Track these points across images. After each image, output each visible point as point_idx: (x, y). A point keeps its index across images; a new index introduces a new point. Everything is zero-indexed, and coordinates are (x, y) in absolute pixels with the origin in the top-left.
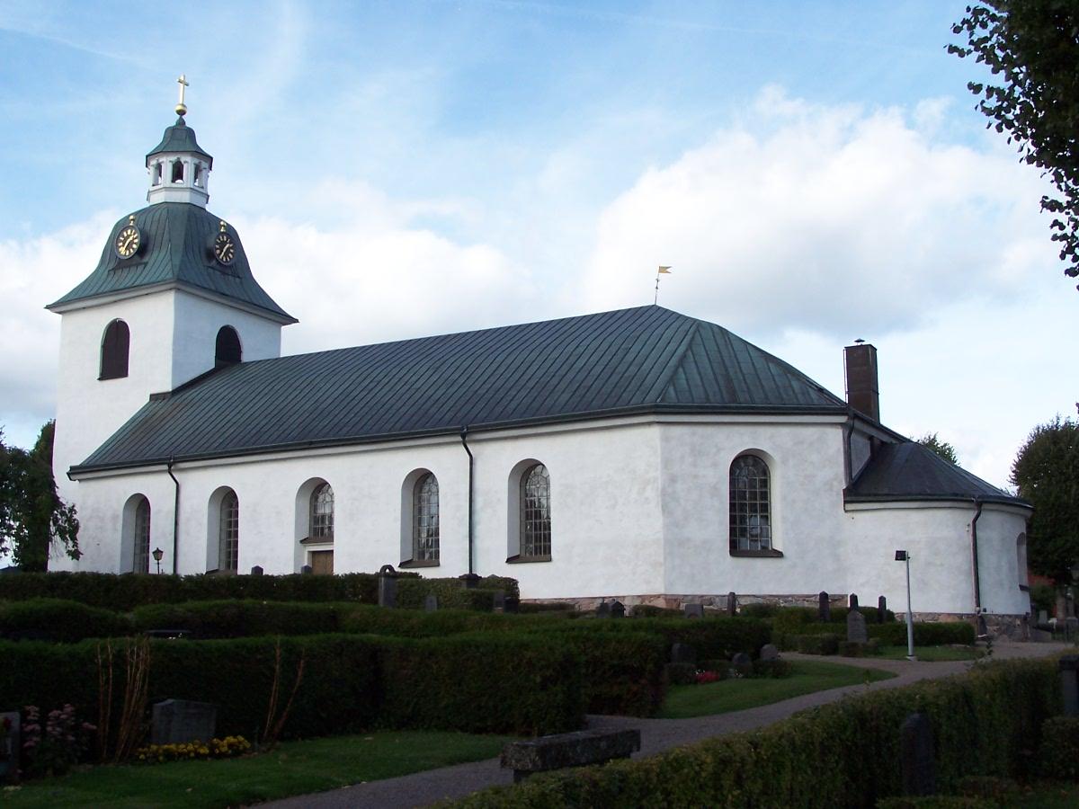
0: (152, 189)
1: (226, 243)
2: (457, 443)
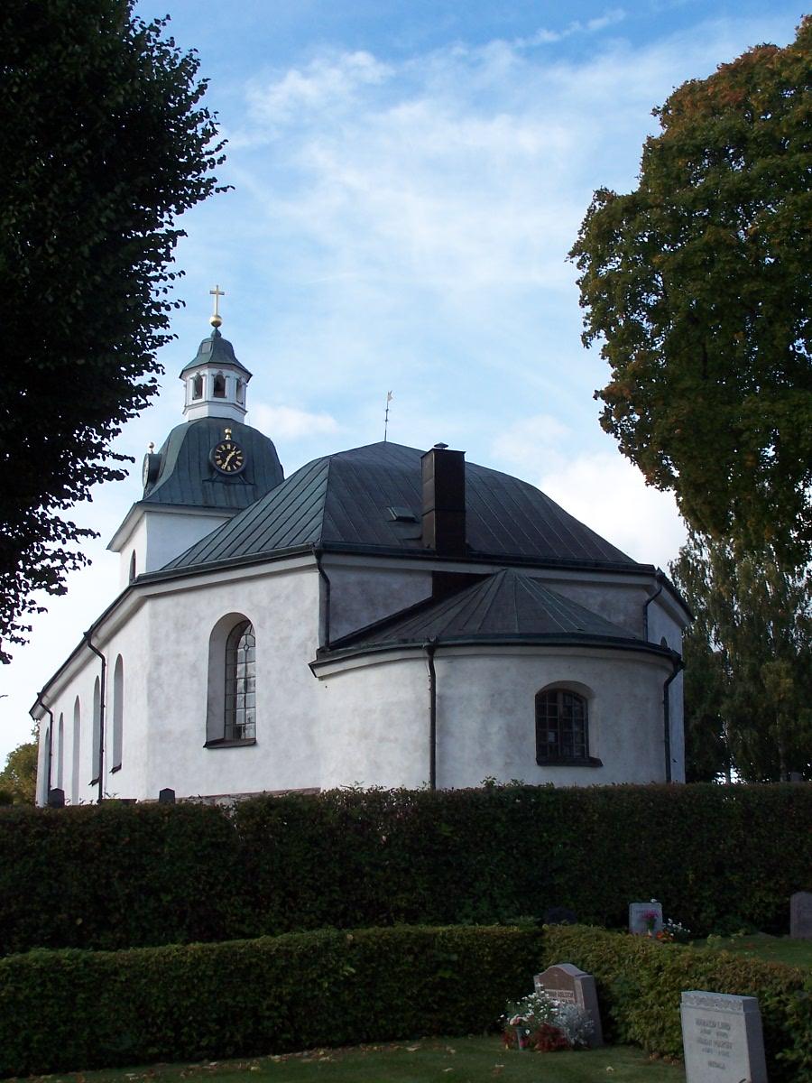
0: (191, 402)
1: (231, 451)
2: (424, 658)
